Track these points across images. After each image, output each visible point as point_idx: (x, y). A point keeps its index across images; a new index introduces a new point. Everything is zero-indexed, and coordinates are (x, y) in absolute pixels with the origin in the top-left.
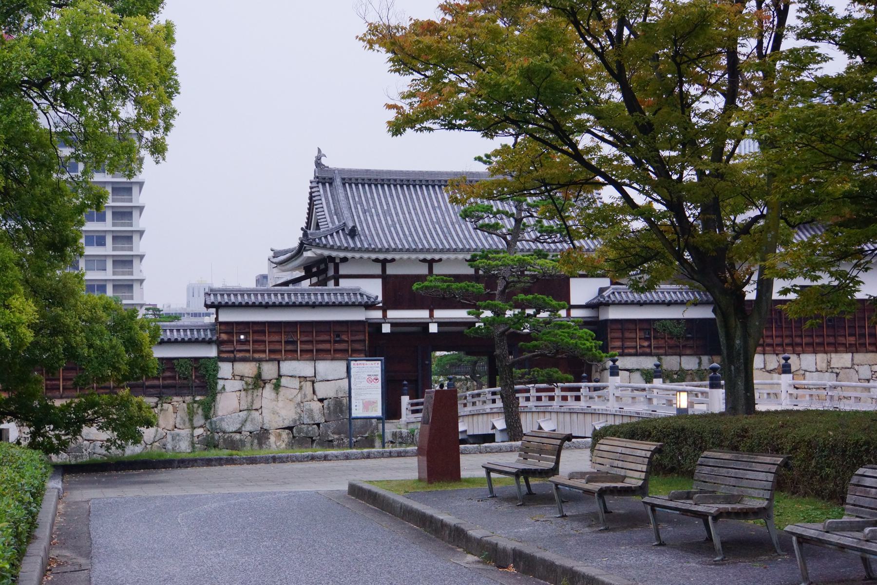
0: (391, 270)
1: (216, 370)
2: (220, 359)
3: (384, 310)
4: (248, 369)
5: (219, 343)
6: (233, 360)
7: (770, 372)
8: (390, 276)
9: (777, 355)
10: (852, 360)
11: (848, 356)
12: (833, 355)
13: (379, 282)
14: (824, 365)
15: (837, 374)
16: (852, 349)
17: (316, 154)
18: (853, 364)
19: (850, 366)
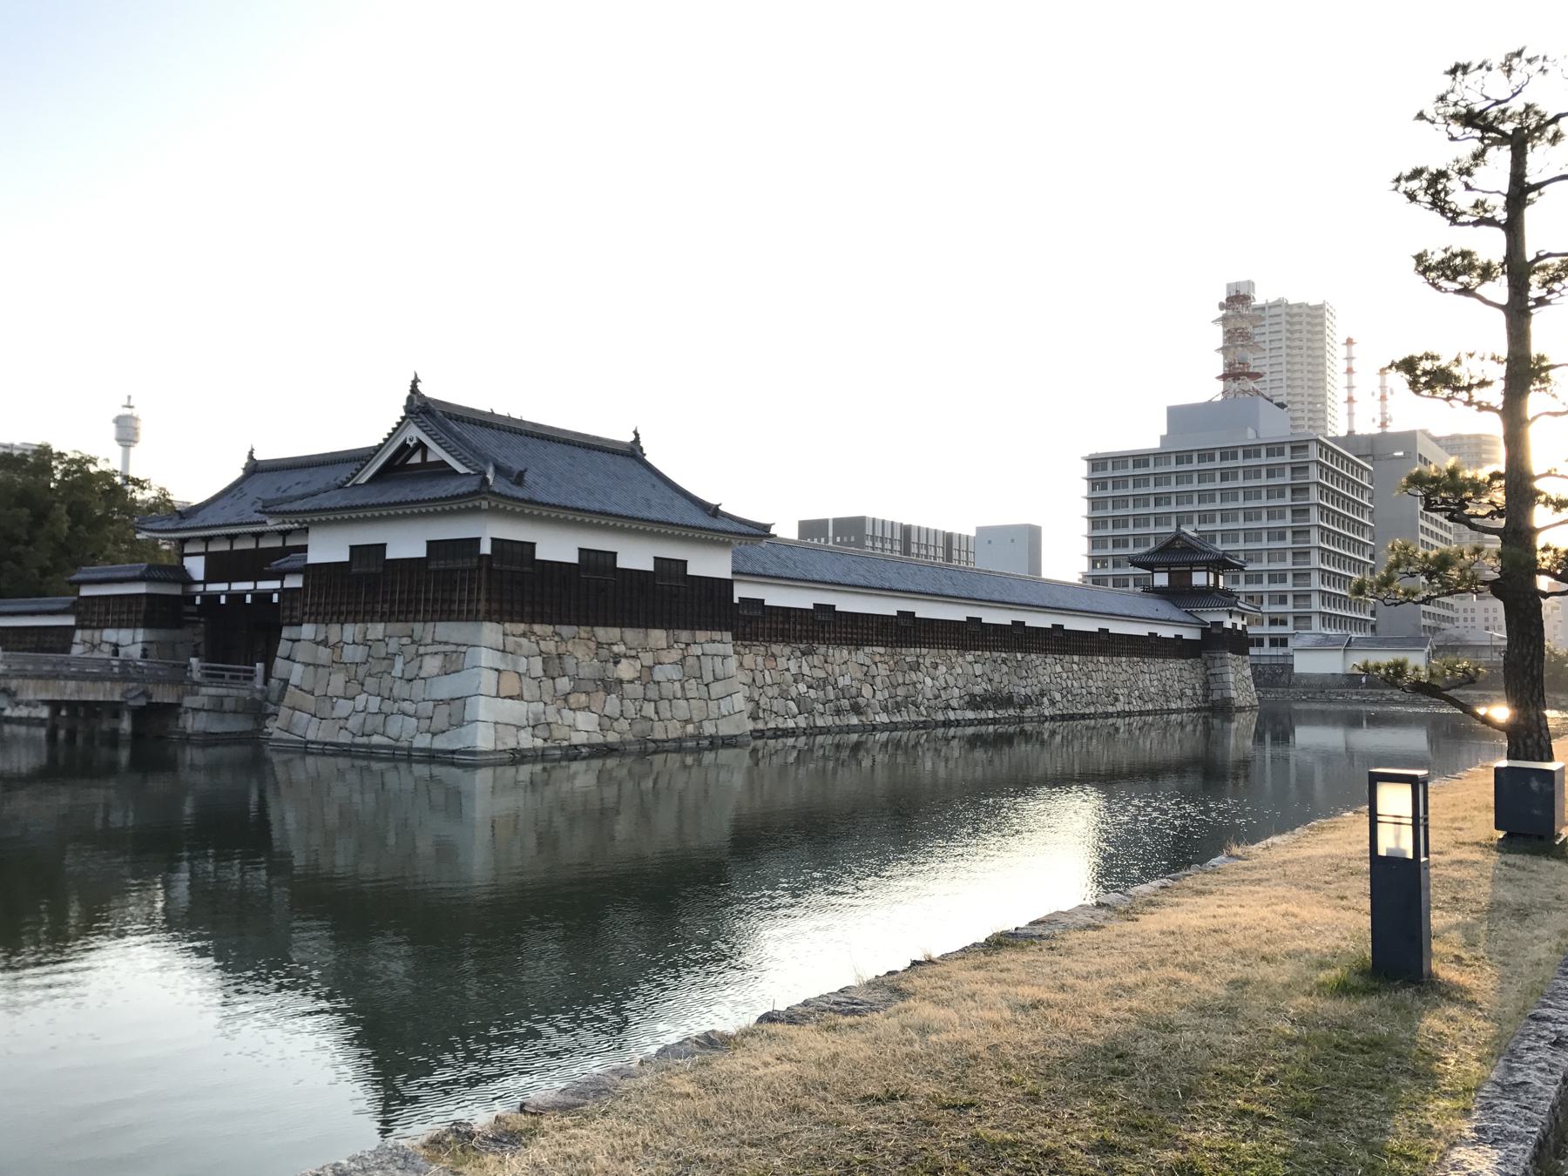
0: (213, 548)
1: (73, 635)
2: (80, 626)
3: (204, 582)
4: (87, 634)
5: (78, 614)
6: (83, 627)
7: (318, 643)
8: (211, 553)
9: (327, 625)
10: (385, 629)
11: (380, 627)
12: (369, 625)
13: (202, 559)
14: (361, 636)
15: (370, 647)
16: (386, 618)
17: (249, 450)
18: (385, 636)
19: (381, 638)
